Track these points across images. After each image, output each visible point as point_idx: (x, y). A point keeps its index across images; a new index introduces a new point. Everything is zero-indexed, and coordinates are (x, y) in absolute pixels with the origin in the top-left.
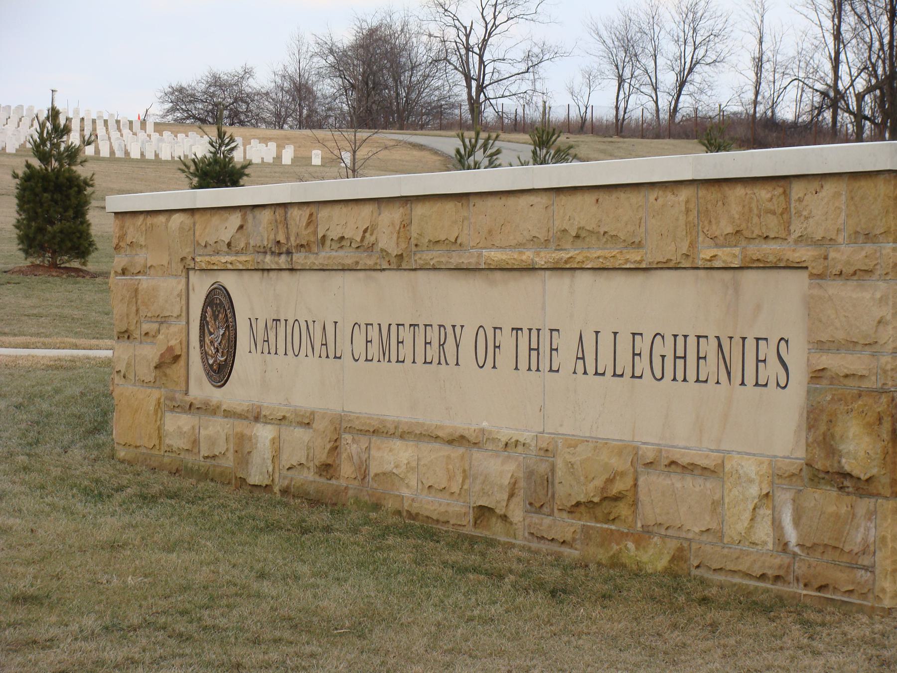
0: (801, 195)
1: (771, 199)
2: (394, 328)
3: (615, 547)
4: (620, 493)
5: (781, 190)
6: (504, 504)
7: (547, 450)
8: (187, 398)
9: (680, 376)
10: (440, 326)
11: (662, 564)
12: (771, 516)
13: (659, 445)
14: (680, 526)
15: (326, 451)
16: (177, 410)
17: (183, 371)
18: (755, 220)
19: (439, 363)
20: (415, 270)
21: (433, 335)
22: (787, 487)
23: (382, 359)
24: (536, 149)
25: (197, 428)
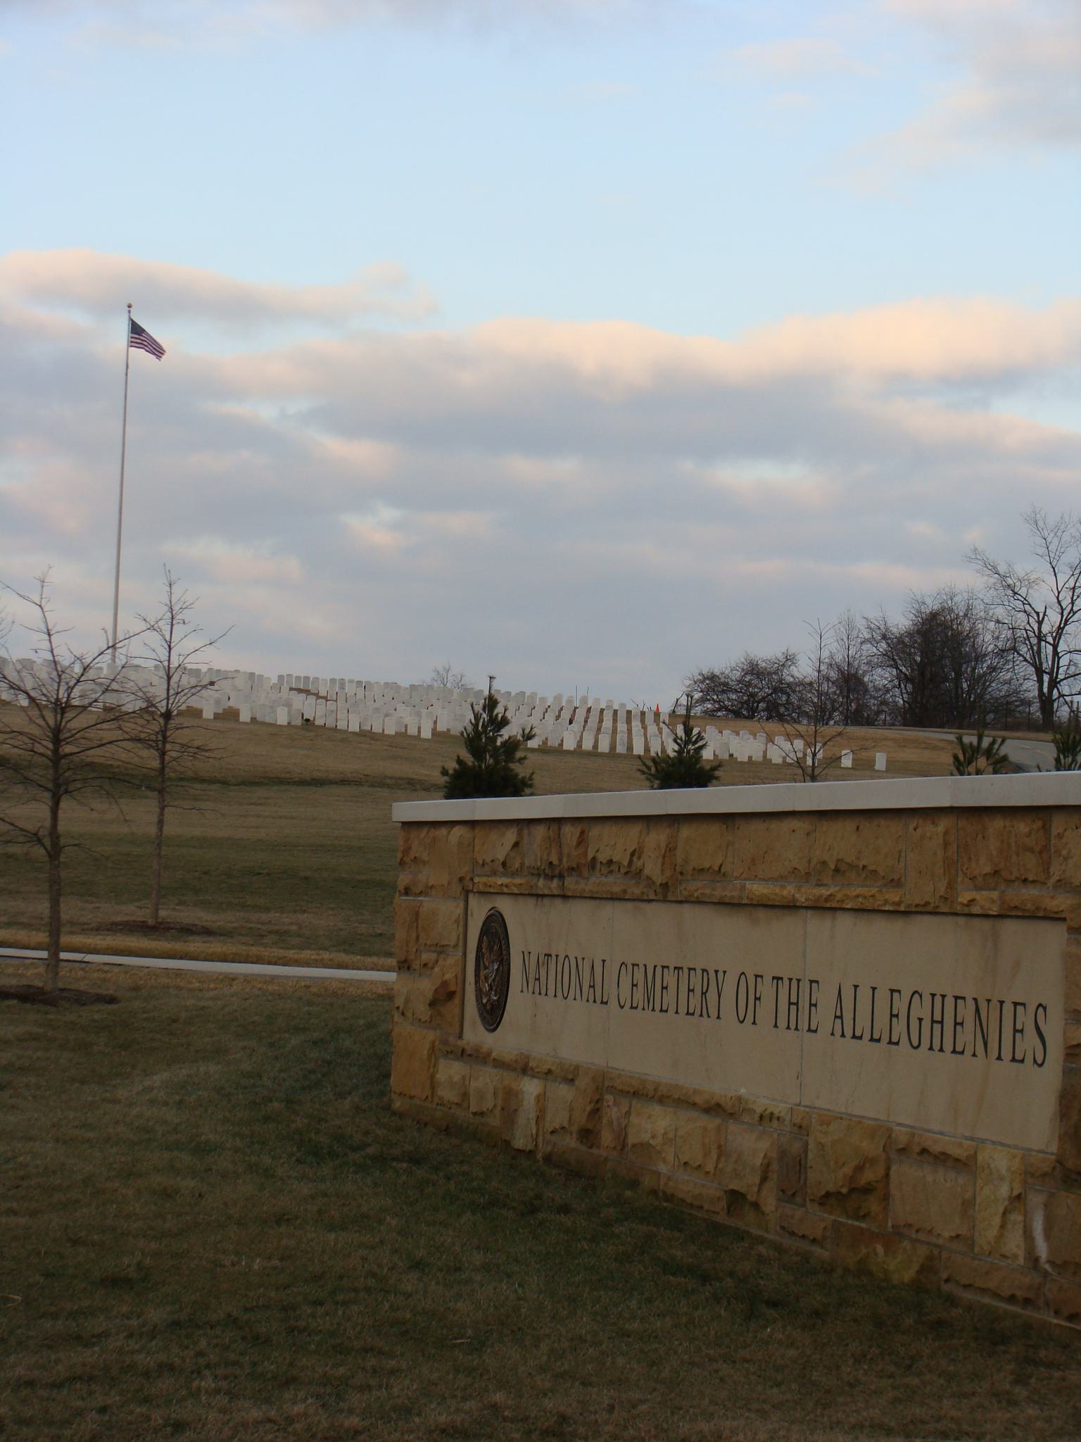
0: (1061, 830)
1: (1030, 833)
2: (659, 970)
3: (864, 1250)
4: (869, 1183)
5: (1040, 823)
6: (756, 1189)
7: (800, 1127)
8: (459, 1043)
9: (936, 1046)
10: (704, 970)
11: (908, 1275)
12: (1022, 1225)
13: (913, 1127)
14: (930, 1228)
15: (586, 1113)
16: (450, 1056)
17: (457, 1011)
18: (1014, 858)
19: (701, 1015)
20: (681, 902)
21: (696, 982)
22: (1040, 1188)
23: (646, 1007)
24: (1059, 756)
25: (468, 1078)
